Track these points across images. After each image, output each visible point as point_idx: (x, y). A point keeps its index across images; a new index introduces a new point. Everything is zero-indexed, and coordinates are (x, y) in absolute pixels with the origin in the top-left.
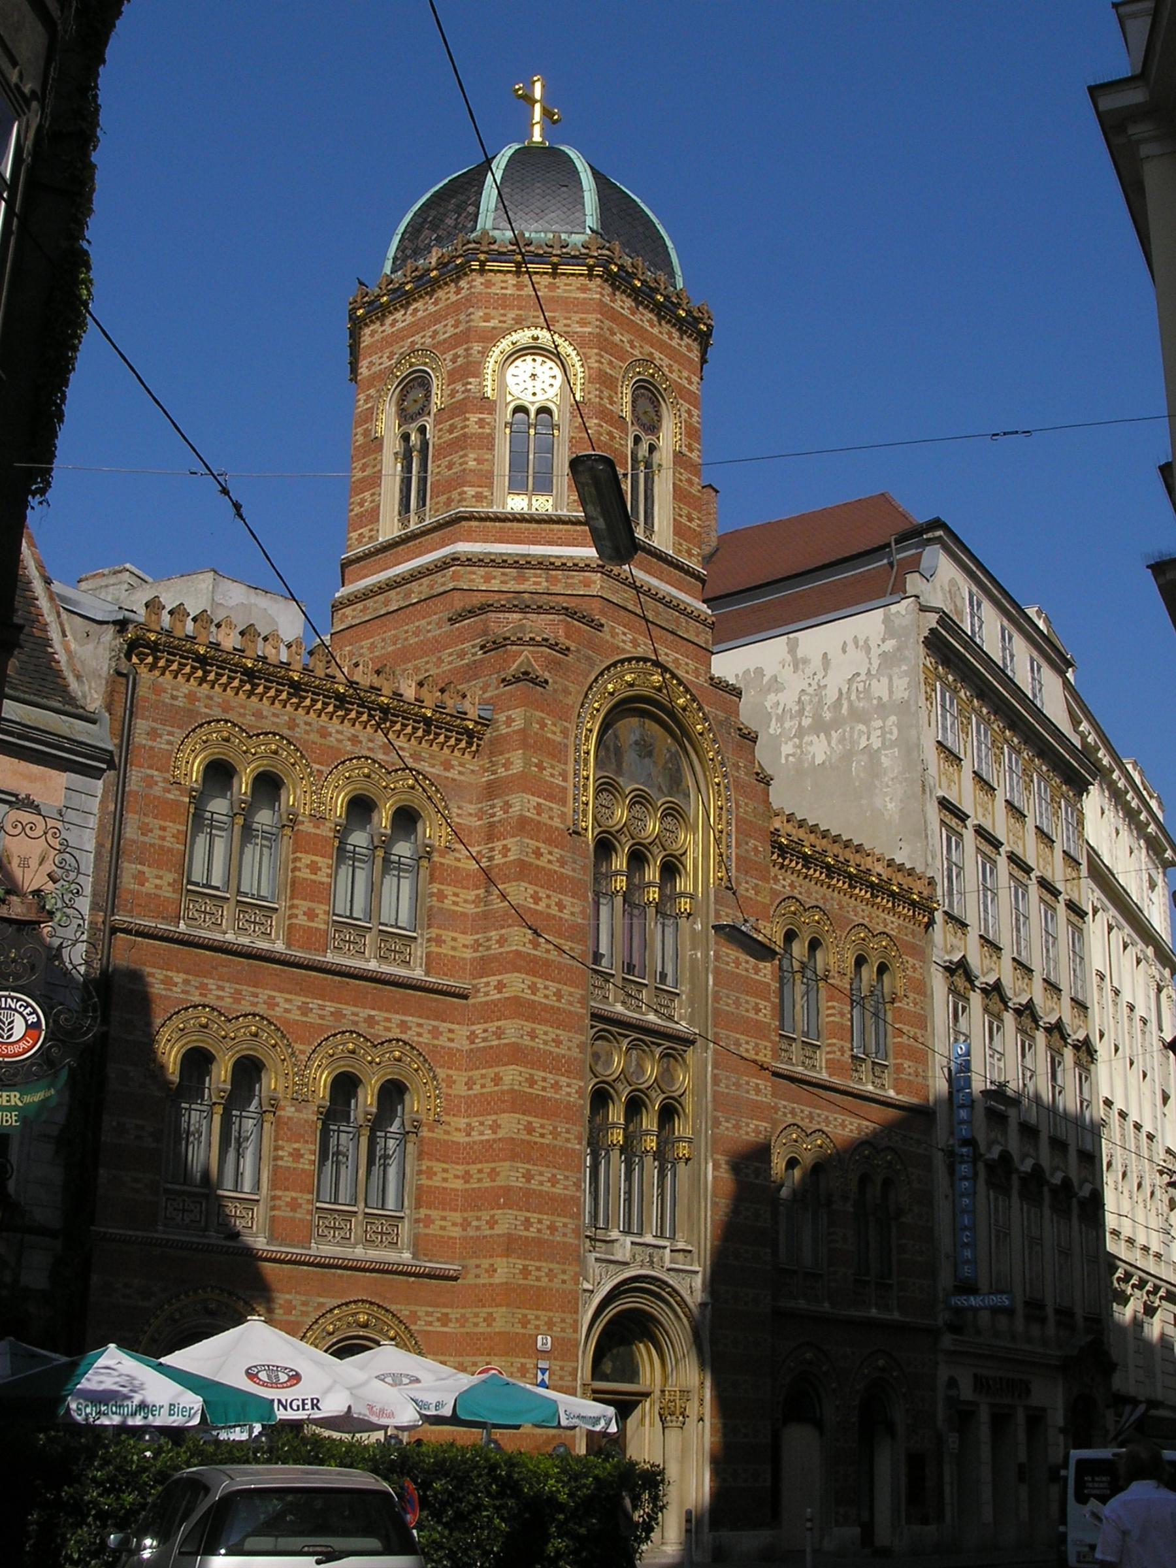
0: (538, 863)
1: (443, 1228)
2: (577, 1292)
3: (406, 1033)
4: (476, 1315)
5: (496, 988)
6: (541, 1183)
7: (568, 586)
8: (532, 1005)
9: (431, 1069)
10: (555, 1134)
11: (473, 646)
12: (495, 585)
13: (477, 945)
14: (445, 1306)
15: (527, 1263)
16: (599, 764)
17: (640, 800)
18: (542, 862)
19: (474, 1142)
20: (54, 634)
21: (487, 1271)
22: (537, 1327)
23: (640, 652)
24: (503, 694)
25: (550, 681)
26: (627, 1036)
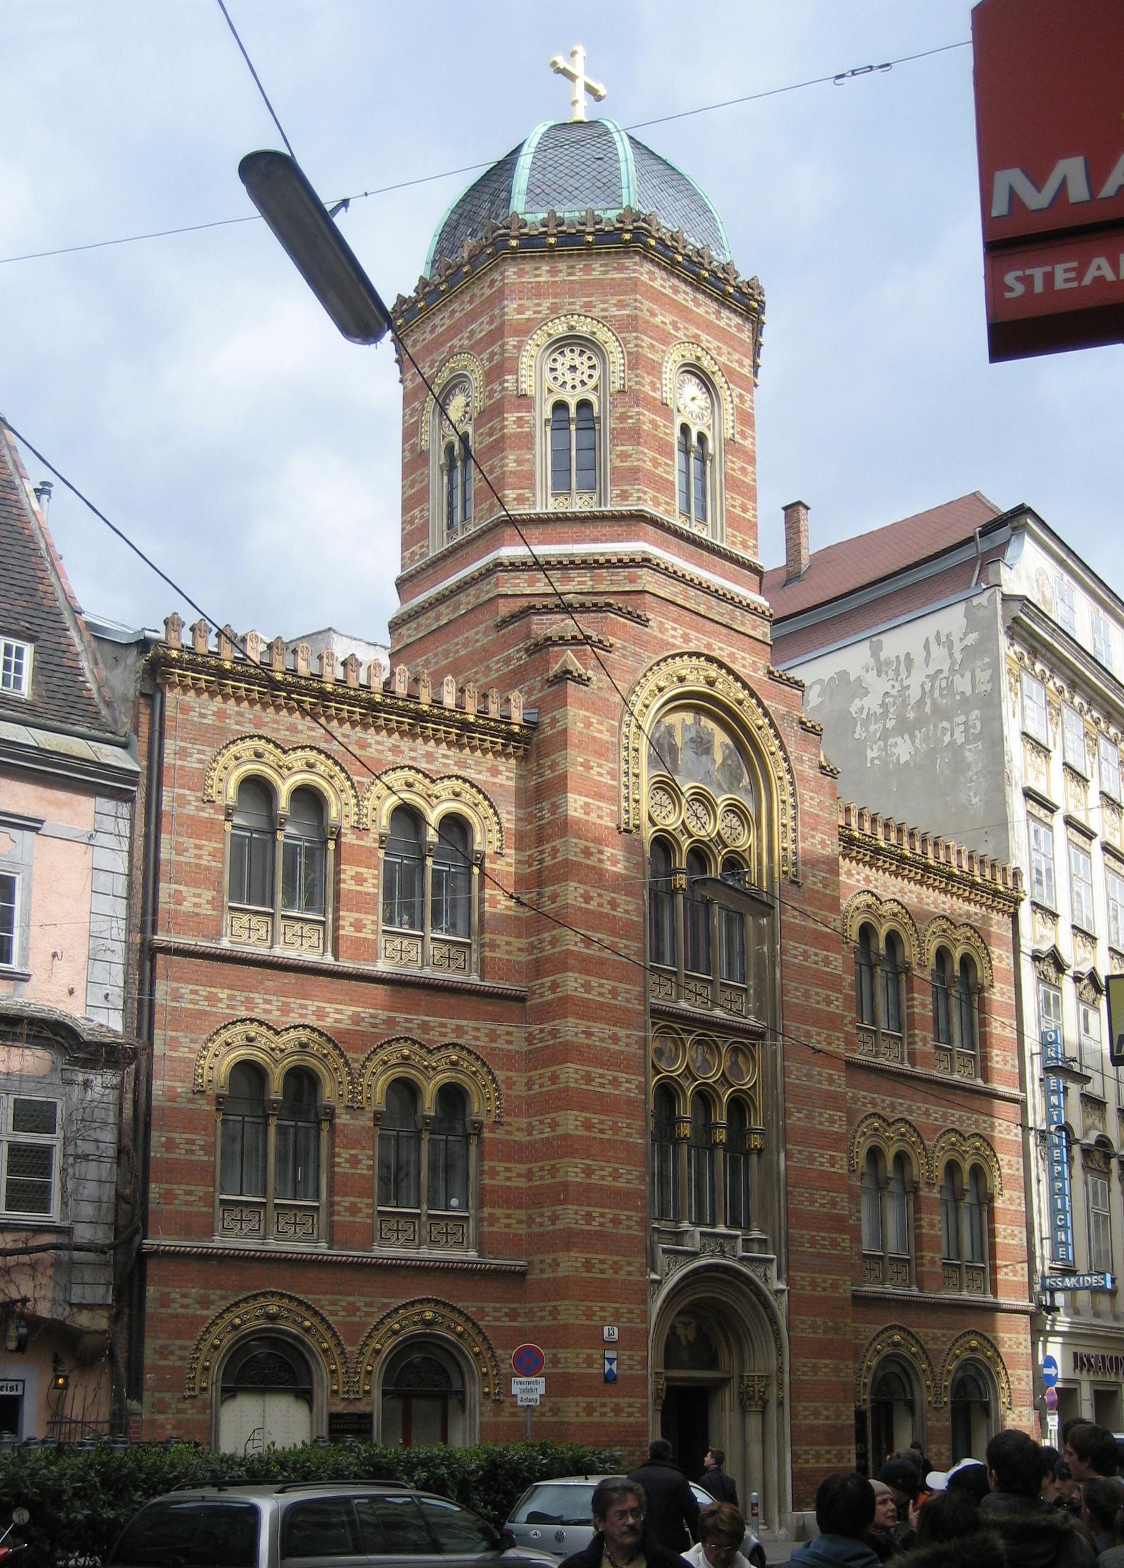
0: (589, 862)
1: (508, 1226)
3: (462, 1037)
4: (542, 1309)
5: (550, 988)
6: (603, 1178)
9: (490, 1072)
10: (616, 1129)
11: (518, 651)
13: (530, 949)
15: (590, 1256)
16: (652, 763)
19: (536, 1141)
21: (551, 1265)
22: (603, 1319)
23: (692, 647)
24: (545, 697)
25: (594, 679)
26: (690, 1032)
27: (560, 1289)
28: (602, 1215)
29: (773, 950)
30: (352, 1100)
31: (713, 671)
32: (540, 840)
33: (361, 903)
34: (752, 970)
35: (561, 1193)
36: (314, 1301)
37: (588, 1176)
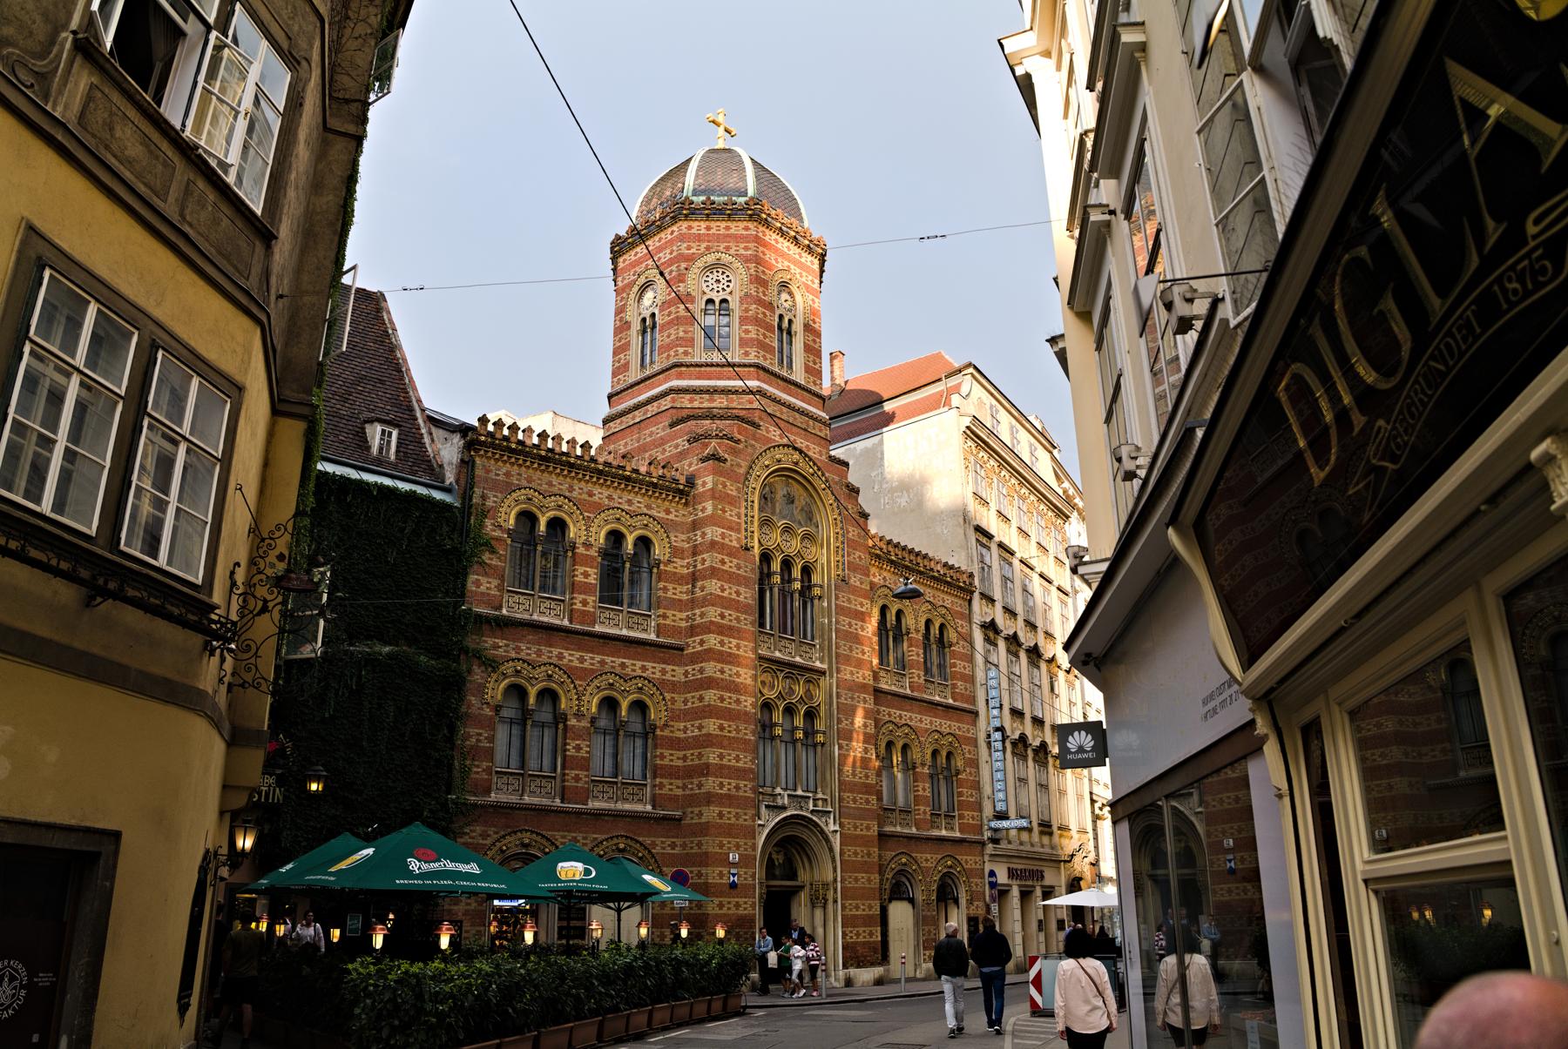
1: (671, 790)
2: (754, 826)
4: (692, 842)
6: (730, 761)
8: (721, 653)
10: (738, 731)
12: (696, 404)
14: (673, 837)
16: (761, 510)
17: (787, 530)
18: (726, 568)
20: (427, 440)
22: (729, 848)
26: (782, 671)
27: (704, 829)
28: (729, 784)
29: (830, 622)
30: (578, 710)
31: (796, 456)
32: (694, 554)
33: (586, 588)
34: (817, 634)
35: (705, 770)
37: (721, 759)
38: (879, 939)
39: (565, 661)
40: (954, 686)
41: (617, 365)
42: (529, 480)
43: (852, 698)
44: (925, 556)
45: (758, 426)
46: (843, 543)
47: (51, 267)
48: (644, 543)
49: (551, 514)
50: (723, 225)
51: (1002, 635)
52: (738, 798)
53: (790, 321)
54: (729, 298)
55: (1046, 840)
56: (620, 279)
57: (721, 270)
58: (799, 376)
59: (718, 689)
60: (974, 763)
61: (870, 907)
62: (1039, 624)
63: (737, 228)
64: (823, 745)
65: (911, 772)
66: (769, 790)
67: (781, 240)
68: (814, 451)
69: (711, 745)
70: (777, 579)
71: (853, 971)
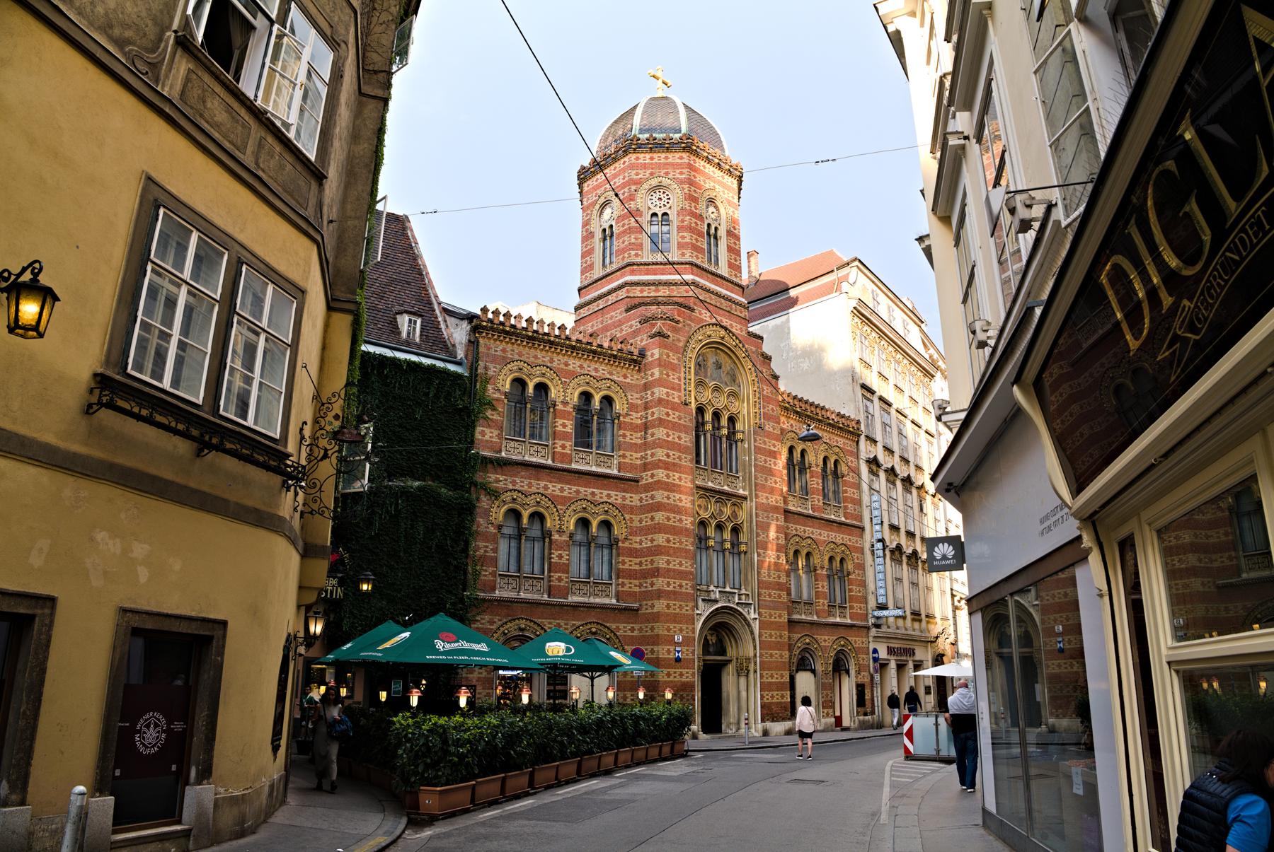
1: (630, 587)
4: (647, 627)
6: (675, 565)
7: (679, 293)
8: (667, 483)
10: (681, 543)
12: (645, 294)
13: (642, 457)
16: (696, 374)
17: (717, 389)
18: (670, 418)
20: (443, 326)
22: (675, 632)
27: (655, 617)
29: (750, 459)
30: (560, 528)
31: (723, 332)
32: (646, 408)
33: (565, 436)
34: (740, 468)
35: (656, 573)
36: (542, 622)
37: (668, 564)
38: (789, 700)
39: (550, 491)
40: (846, 507)
41: (584, 265)
42: (520, 354)
43: (768, 517)
44: (823, 408)
45: (693, 310)
46: (759, 398)
47: (164, 207)
48: (608, 400)
49: (537, 380)
50: (663, 155)
51: (883, 468)
52: (681, 593)
53: (716, 229)
54: (669, 212)
55: (916, 625)
56: (585, 200)
57: (662, 191)
58: (723, 270)
59: (665, 511)
60: (862, 567)
61: (782, 676)
62: (911, 459)
63: (674, 157)
64: (745, 553)
65: (813, 574)
66: (704, 588)
67: (708, 166)
68: (736, 328)
69: (661, 554)
70: (709, 427)
71: (769, 725)
